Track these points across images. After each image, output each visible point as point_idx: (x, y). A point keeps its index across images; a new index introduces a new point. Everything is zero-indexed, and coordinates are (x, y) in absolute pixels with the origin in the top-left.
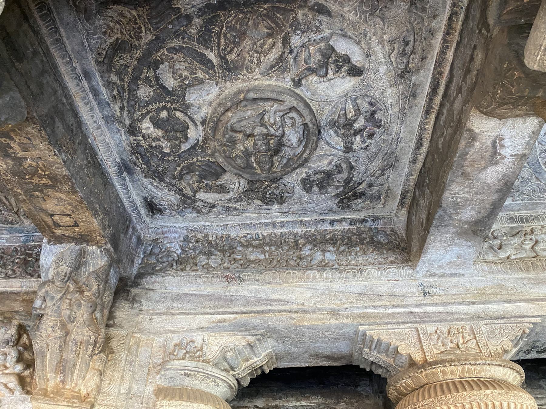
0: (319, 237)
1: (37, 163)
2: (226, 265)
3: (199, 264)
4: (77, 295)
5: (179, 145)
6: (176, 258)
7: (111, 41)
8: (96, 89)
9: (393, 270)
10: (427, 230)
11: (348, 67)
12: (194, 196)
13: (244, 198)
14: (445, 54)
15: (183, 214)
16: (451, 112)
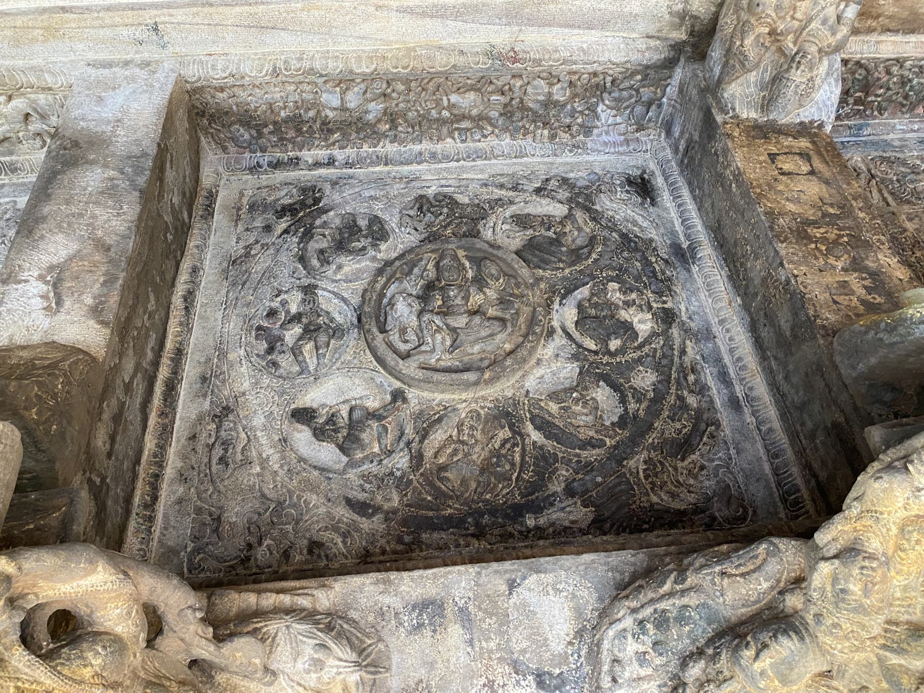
0: (354, 135)
2: (519, 83)
3: (566, 85)
4: (782, 27)
5: (593, 295)
6: (605, 95)
7: (693, 457)
8: (722, 383)
9: (218, 74)
10: (162, 150)
11: (316, 423)
12: (571, 209)
13: (487, 207)
14: (157, 445)
15: (591, 177)
16: (140, 353)
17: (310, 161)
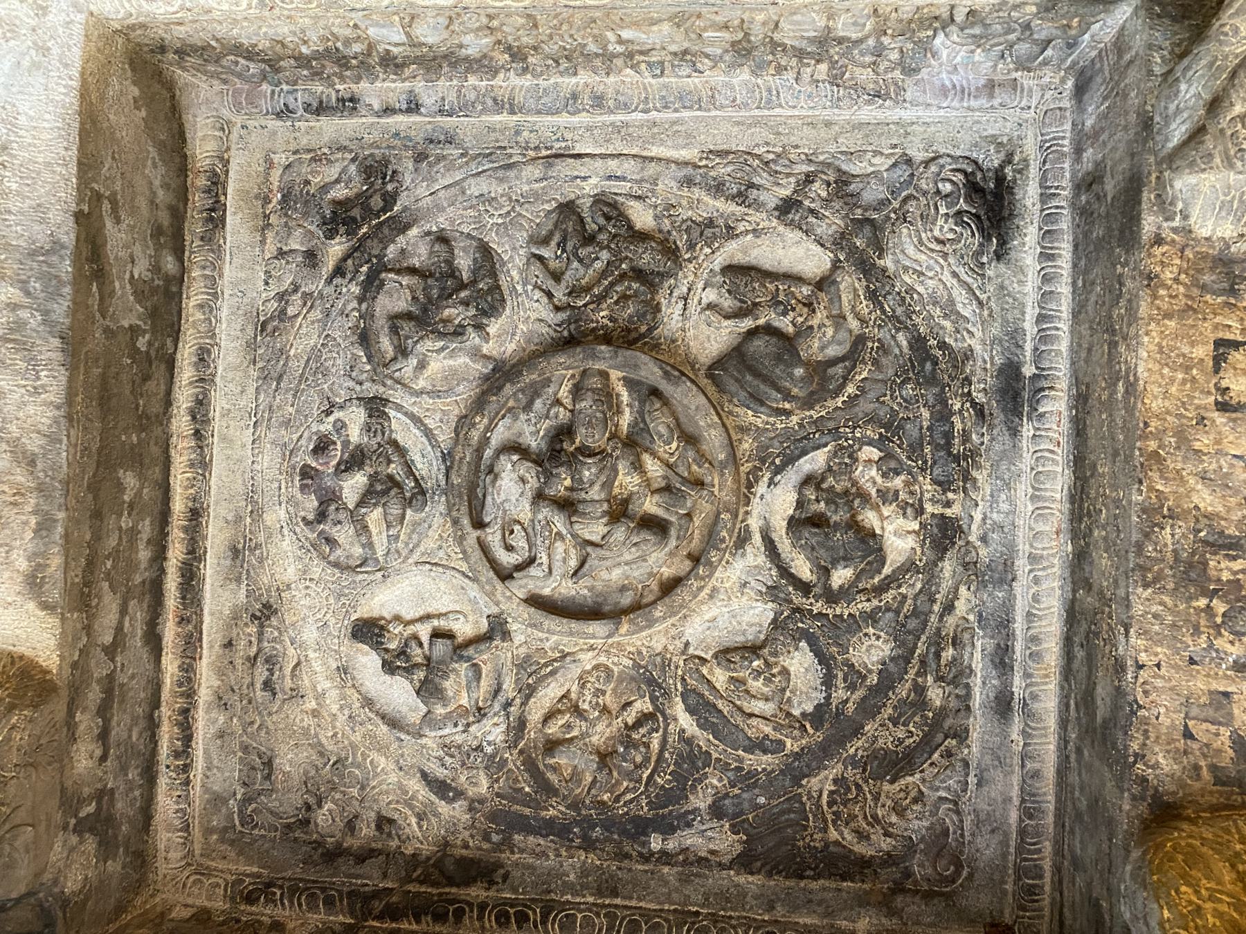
1: (1211, 646)
7: (910, 779)
8: (996, 667)
17: (376, 107)
